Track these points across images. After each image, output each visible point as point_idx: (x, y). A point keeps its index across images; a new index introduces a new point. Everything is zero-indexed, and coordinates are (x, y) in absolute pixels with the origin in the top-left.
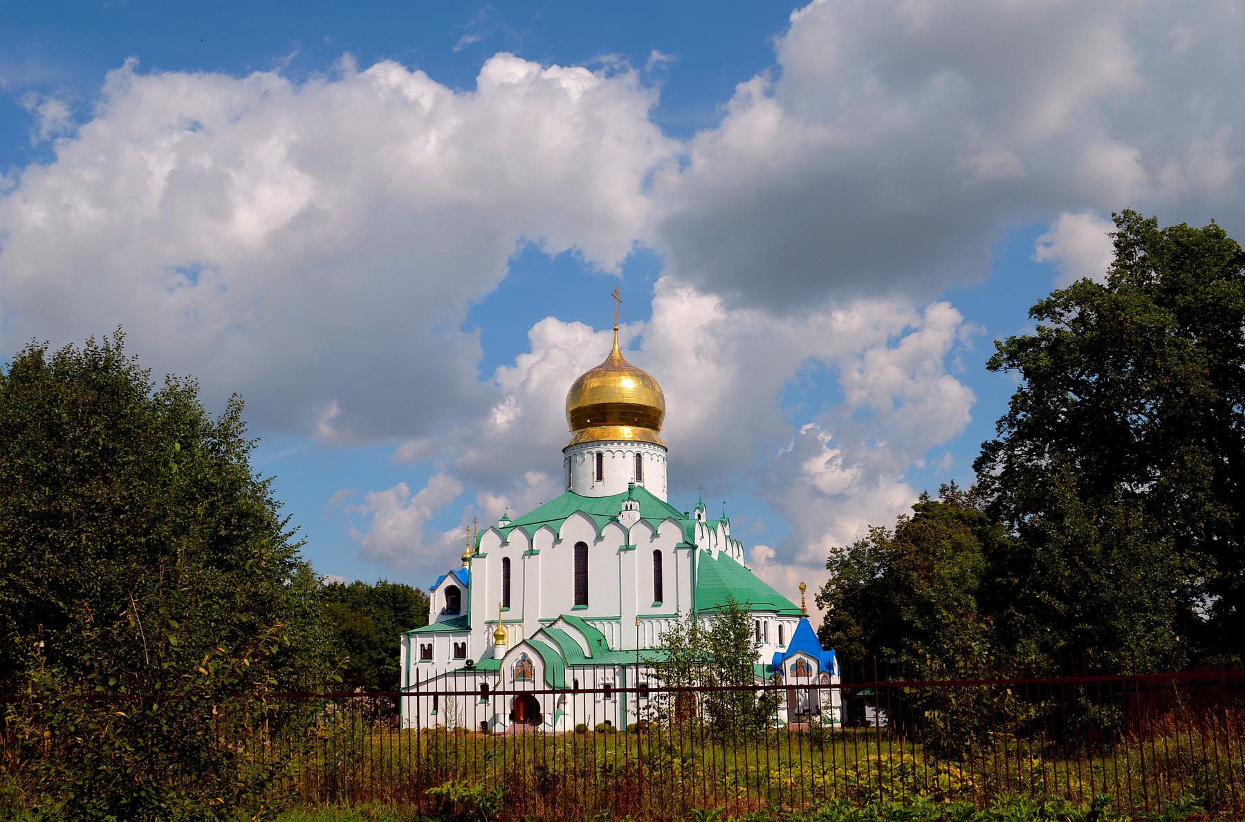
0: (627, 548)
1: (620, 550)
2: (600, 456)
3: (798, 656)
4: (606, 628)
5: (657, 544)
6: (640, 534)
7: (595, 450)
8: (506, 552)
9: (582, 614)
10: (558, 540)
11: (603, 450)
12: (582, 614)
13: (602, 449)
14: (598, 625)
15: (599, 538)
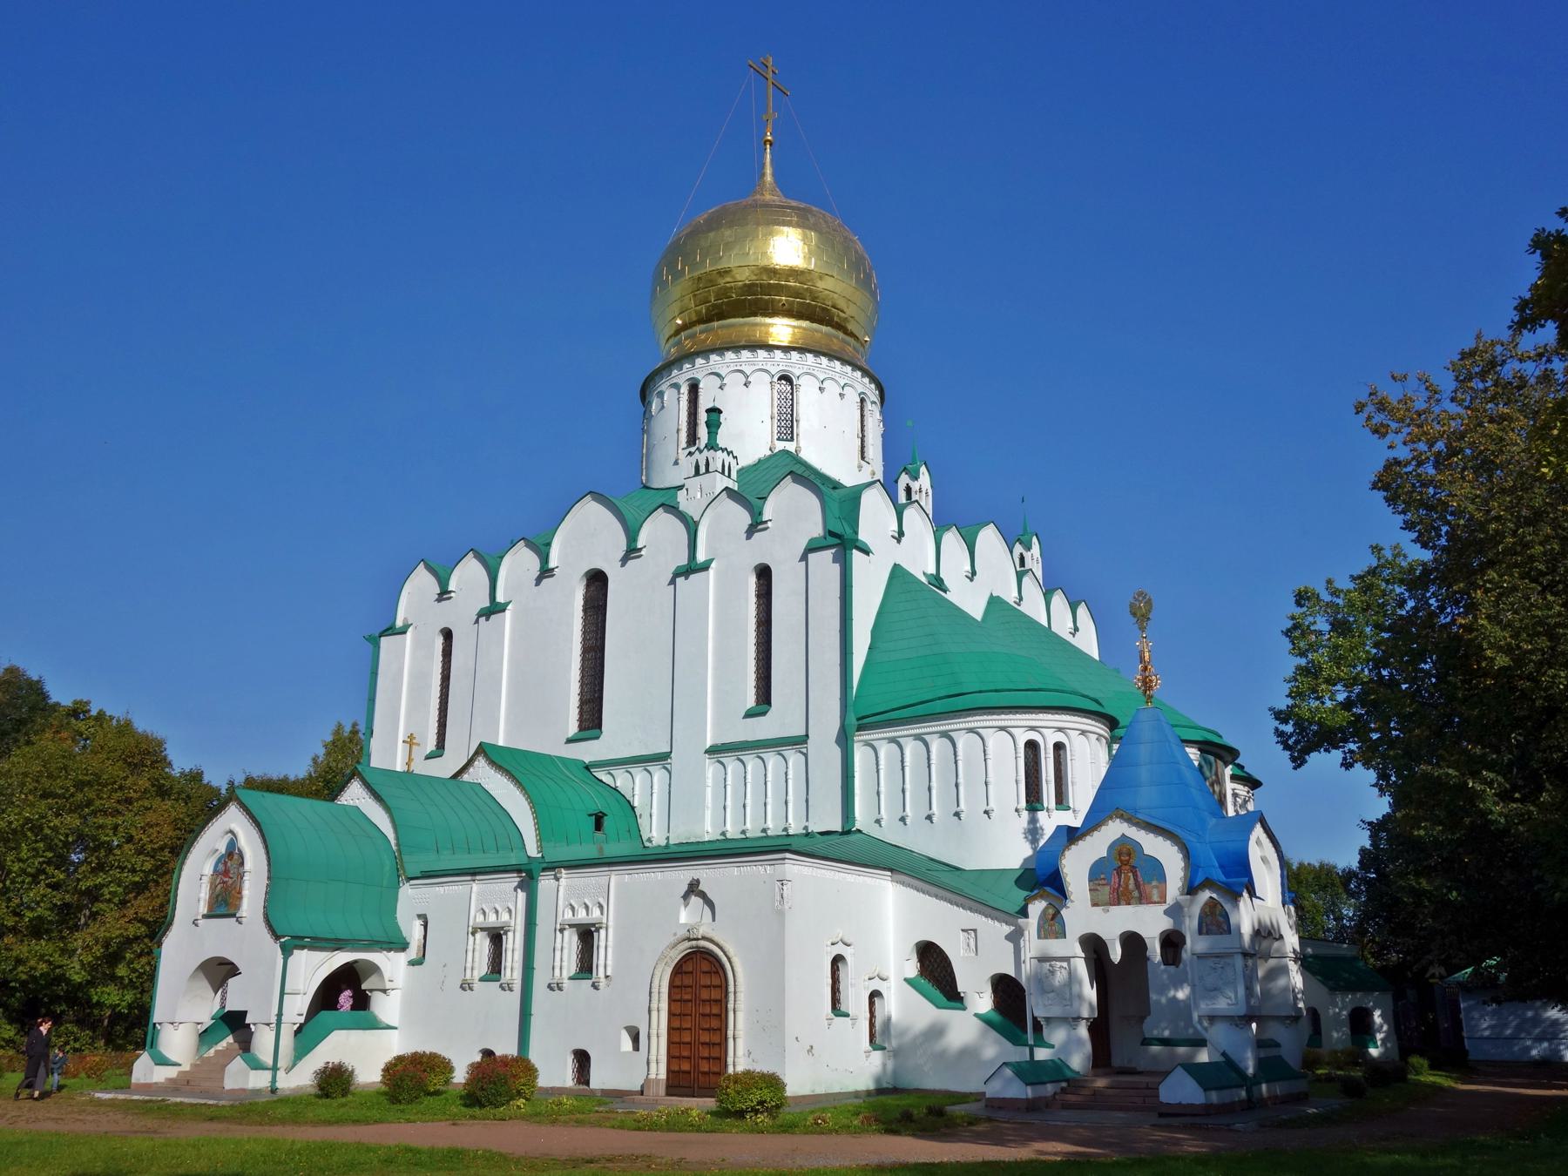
0: (692, 568)
1: (677, 574)
2: (694, 388)
3: (1115, 829)
4: (636, 785)
5: (763, 549)
6: (722, 524)
7: (682, 376)
8: (446, 615)
9: (588, 752)
10: (546, 572)
11: (699, 376)
12: (588, 752)
13: (698, 368)
14: (620, 779)
15: (632, 552)
